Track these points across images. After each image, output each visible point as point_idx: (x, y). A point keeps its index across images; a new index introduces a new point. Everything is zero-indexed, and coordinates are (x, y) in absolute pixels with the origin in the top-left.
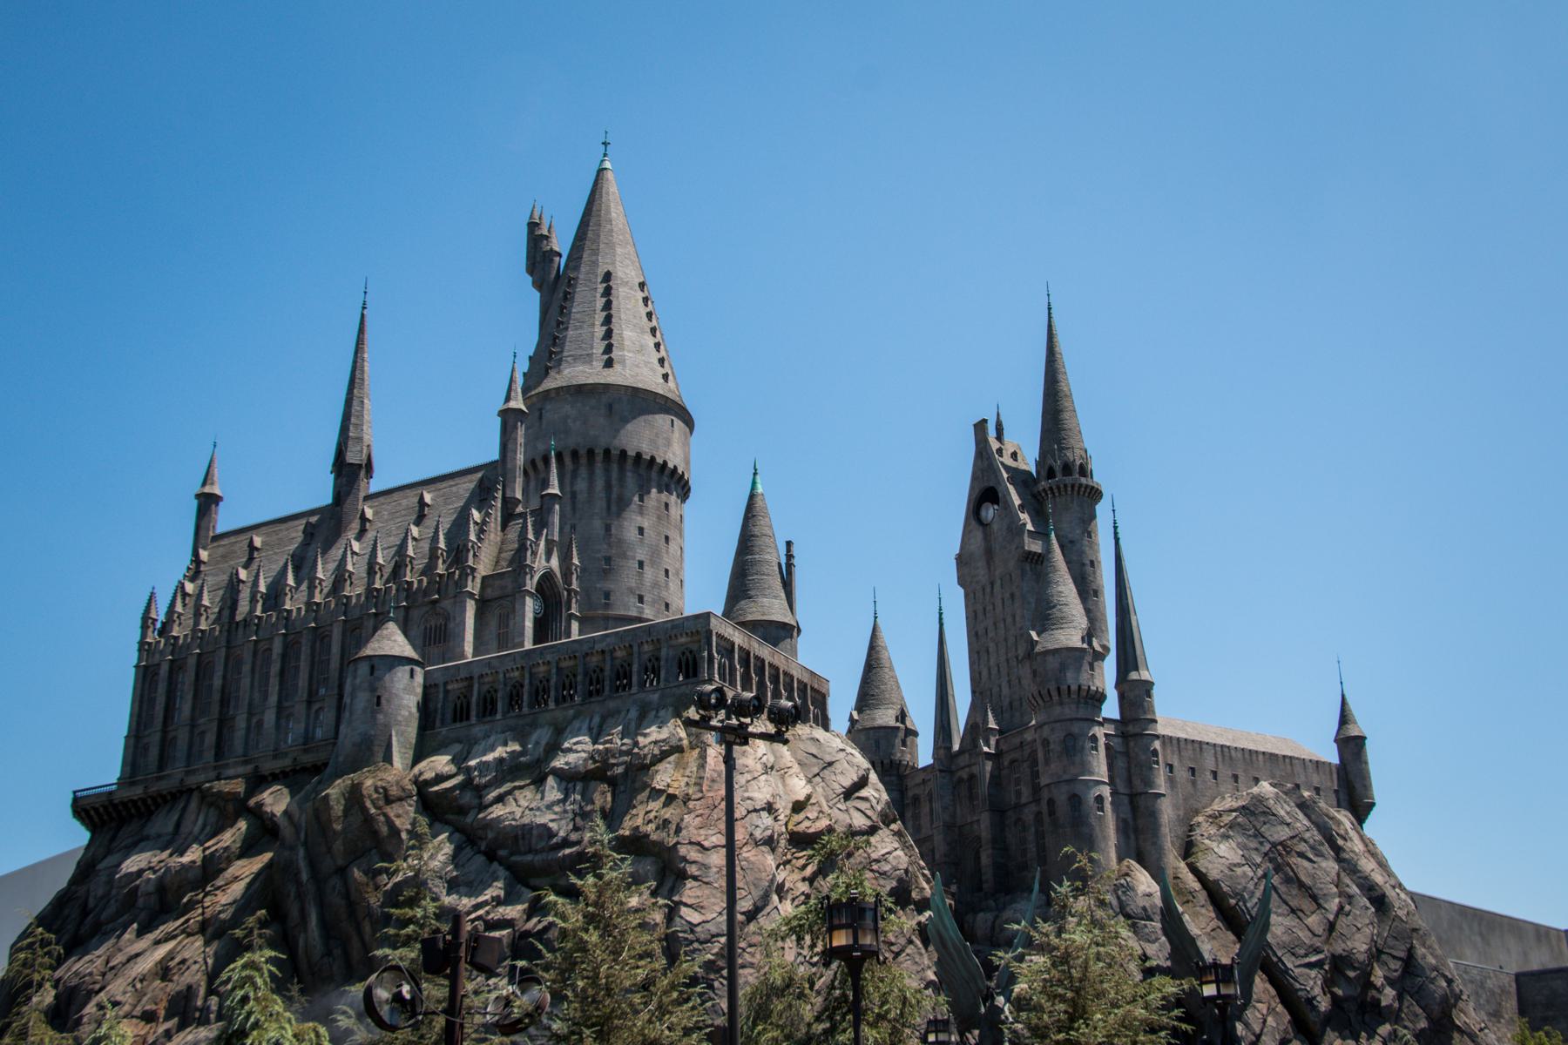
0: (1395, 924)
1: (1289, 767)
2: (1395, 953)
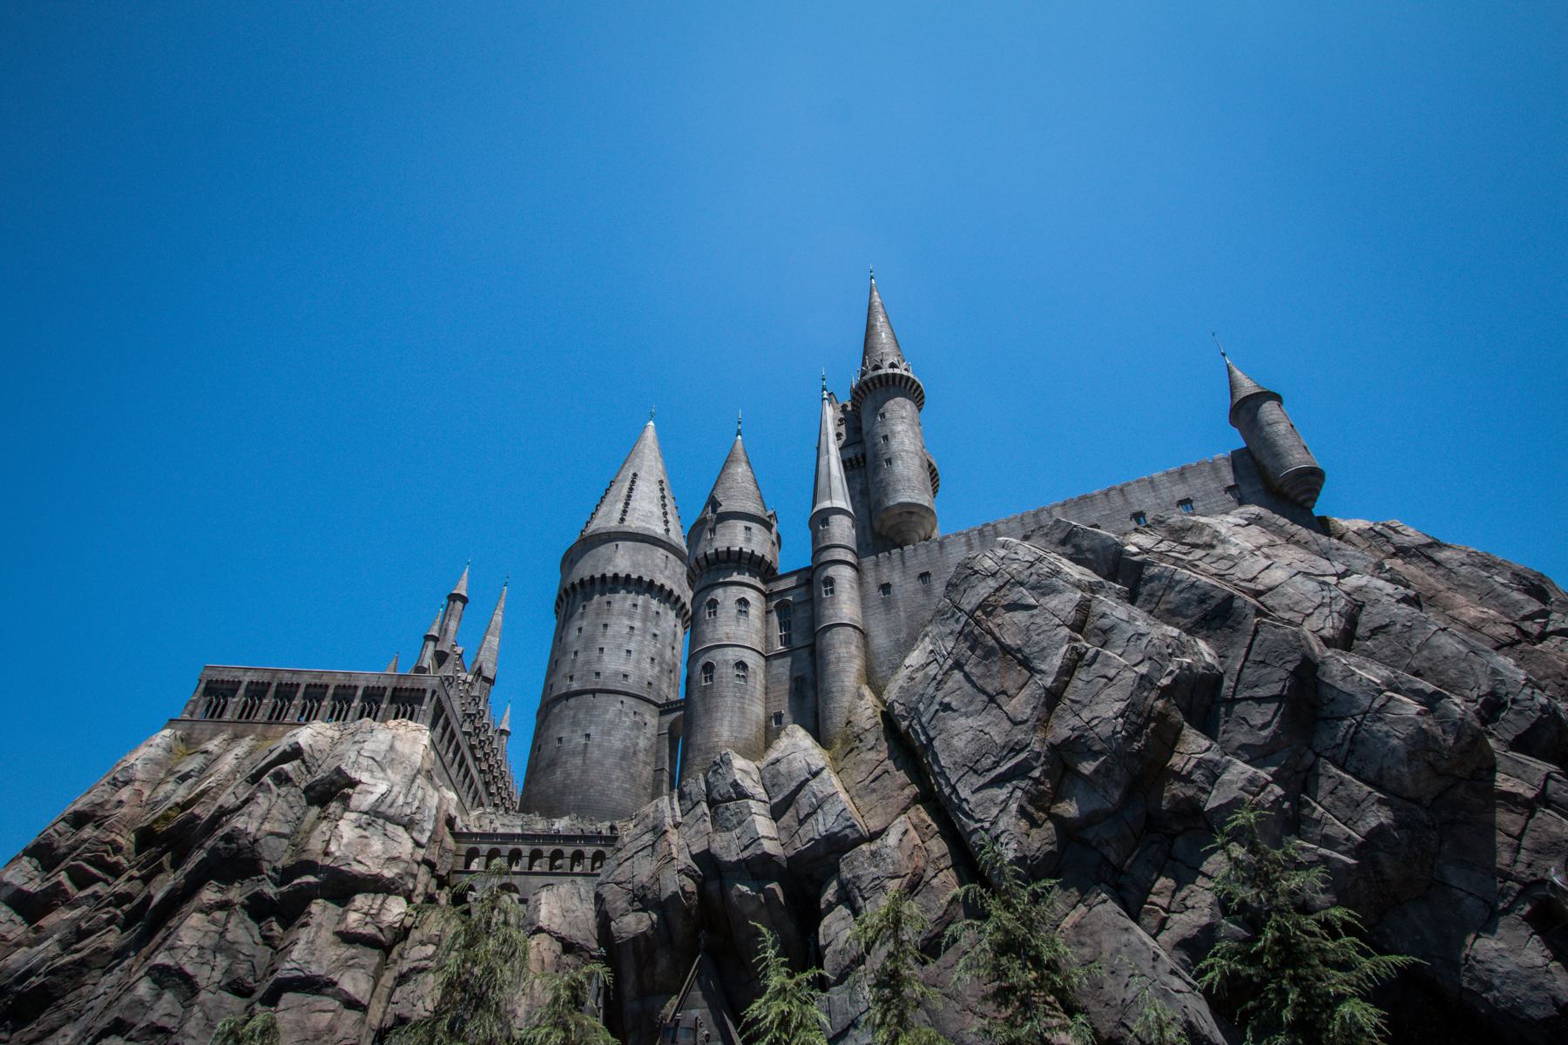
0: (1259, 638)
2: (1260, 692)
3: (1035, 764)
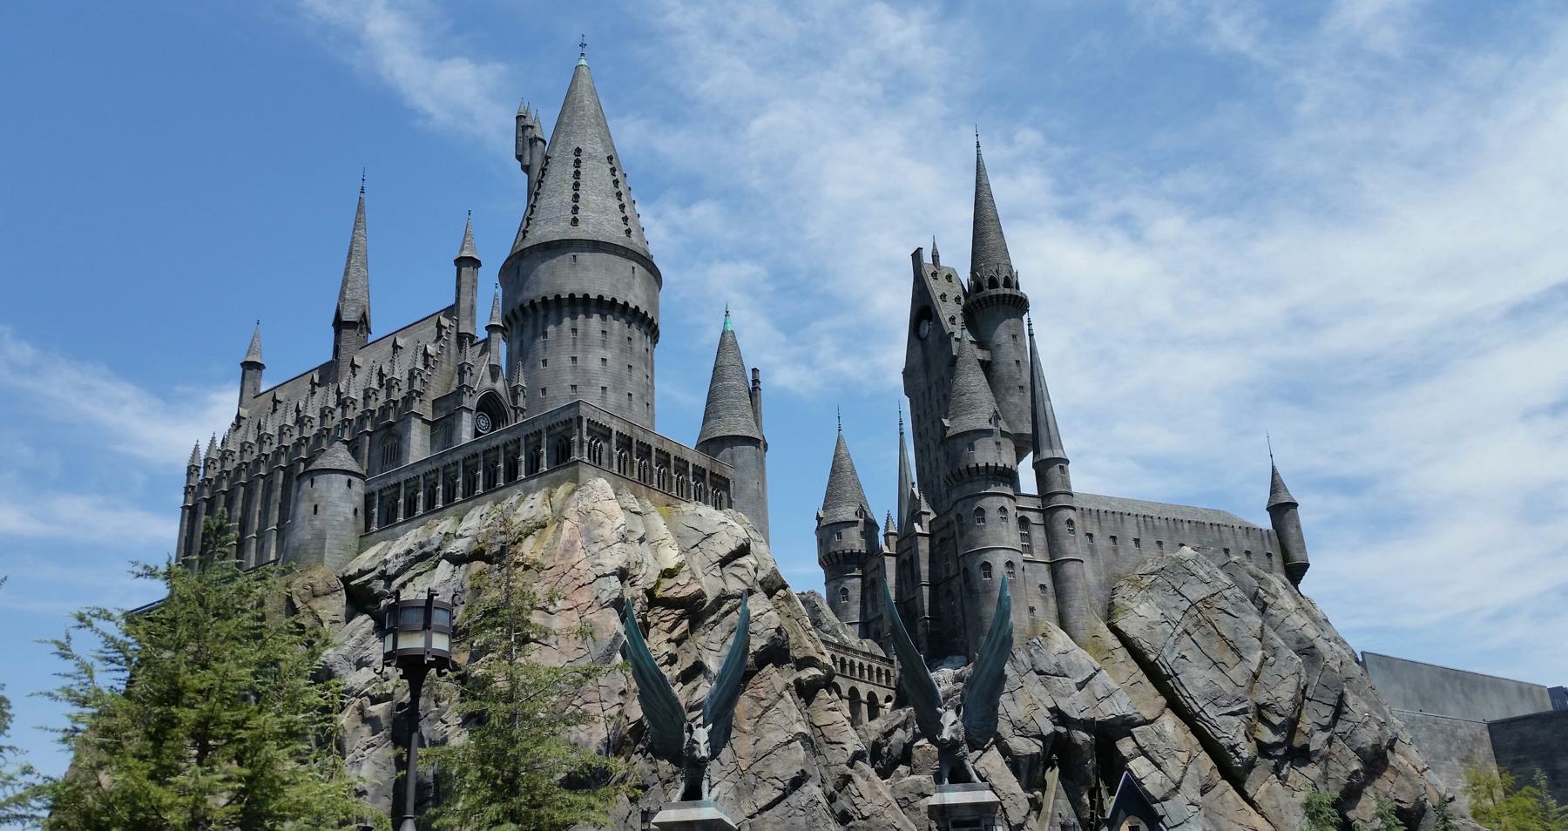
0: (1324, 673)
1: (1217, 534)
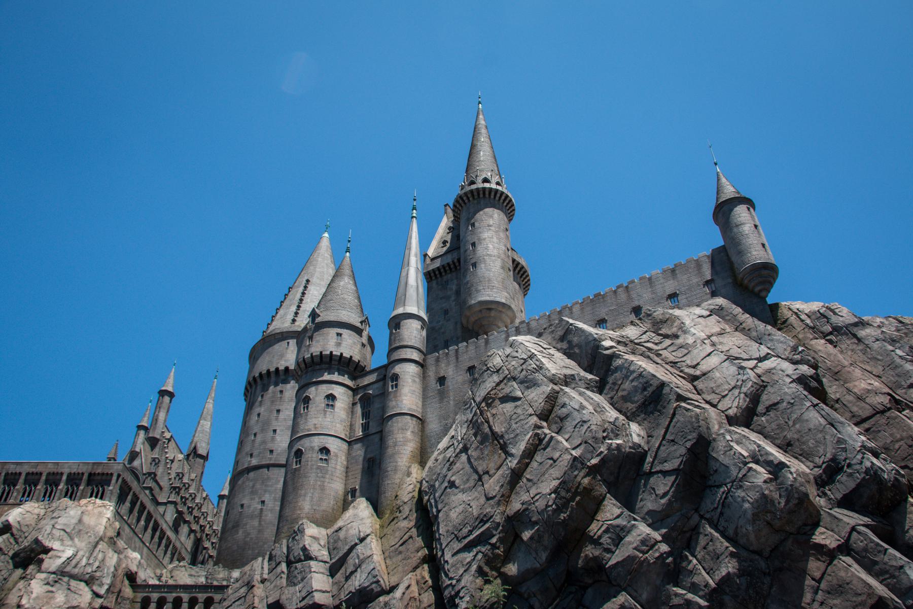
0: (675, 420)
3: (494, 532)
